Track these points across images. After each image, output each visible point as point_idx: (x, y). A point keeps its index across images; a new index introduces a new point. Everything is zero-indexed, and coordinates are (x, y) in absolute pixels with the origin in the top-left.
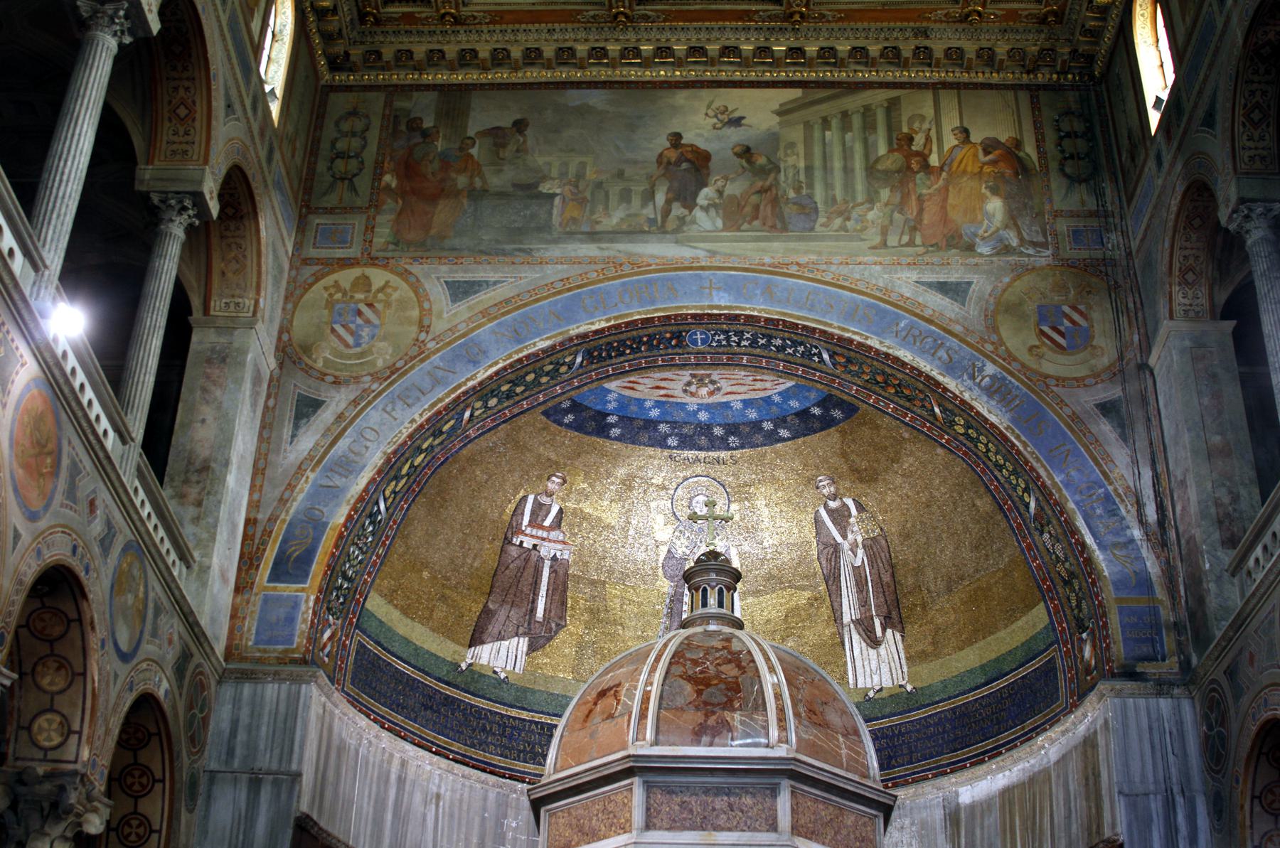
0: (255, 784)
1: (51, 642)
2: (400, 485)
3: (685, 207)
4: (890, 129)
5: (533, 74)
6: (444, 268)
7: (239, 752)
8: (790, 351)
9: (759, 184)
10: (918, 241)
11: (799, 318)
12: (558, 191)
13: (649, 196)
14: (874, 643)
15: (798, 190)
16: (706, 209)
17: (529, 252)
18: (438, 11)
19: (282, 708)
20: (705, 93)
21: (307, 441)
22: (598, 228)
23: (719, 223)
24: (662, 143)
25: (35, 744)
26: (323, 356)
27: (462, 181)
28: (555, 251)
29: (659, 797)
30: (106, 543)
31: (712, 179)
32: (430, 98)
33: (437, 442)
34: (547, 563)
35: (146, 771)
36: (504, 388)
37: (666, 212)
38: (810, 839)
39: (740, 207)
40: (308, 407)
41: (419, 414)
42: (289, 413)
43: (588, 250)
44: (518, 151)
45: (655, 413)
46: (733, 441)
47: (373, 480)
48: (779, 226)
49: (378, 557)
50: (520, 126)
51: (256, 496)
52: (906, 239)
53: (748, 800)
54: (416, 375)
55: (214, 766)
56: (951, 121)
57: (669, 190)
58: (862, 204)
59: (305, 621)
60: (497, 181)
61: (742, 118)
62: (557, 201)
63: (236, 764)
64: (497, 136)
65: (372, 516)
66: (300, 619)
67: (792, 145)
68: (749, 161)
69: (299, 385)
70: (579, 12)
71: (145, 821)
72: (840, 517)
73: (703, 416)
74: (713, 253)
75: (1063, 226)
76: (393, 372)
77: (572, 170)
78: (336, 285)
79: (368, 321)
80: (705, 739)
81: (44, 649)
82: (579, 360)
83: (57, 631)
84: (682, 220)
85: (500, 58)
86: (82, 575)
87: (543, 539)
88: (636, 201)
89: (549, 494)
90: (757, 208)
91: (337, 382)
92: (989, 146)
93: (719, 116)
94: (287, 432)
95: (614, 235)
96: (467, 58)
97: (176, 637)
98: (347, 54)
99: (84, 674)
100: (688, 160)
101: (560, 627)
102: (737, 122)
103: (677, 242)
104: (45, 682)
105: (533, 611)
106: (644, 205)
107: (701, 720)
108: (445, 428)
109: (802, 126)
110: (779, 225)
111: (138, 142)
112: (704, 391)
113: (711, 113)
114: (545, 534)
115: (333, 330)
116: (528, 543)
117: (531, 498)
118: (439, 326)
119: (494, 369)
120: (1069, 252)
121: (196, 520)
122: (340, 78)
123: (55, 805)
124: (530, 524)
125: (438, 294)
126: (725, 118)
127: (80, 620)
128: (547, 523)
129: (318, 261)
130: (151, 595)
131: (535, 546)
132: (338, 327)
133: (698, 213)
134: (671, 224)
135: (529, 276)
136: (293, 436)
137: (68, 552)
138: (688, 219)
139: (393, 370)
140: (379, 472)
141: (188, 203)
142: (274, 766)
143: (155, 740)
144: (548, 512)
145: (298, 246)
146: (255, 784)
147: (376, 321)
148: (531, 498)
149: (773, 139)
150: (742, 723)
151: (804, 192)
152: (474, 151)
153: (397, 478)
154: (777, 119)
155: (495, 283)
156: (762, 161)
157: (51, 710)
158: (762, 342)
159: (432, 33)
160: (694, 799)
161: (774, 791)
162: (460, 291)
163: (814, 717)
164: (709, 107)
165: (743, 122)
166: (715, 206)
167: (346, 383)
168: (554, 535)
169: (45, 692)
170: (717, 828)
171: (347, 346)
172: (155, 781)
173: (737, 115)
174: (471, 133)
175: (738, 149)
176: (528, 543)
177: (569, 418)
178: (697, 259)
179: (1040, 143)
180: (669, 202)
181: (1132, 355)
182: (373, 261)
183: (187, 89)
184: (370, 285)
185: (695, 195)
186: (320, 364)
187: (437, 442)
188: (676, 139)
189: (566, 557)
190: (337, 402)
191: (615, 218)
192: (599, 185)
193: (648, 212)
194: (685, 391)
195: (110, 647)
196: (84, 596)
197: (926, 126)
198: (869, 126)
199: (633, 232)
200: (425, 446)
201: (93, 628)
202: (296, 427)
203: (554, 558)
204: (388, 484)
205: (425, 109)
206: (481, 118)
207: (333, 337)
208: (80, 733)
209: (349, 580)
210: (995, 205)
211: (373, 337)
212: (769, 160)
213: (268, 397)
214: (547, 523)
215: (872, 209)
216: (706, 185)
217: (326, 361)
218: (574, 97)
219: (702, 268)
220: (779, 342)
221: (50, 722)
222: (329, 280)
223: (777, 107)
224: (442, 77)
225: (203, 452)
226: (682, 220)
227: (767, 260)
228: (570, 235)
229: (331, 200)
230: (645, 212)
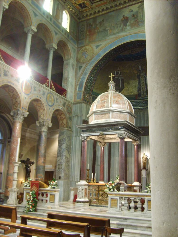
0: (78, 117)
1: (40, 106)
2: (94, 75)
5: (105, 12)
6: (95, 44)
7: (76, 113)
8: (142, 44)
9: (135, 20)
11: (142, 39)
12: (108, 29)
13: (120, 26)
15: (141, 19)
16: (128, 26)
17: (105, 39)
18: (89, 8)
19: (80, 107)
20: (128, 8)
21: (81, 72)
22: (114, 33)
23: (130, 28)
24: (122, 17)
25: (41, 118)
26: (82, 60)
27: (96, 31)
28: (109, 38)
29: (96, 116)
30: (44, 94)
31: (129, 21)
32: (92, 20)
33: (98, 68)
34: (120, 80)
35: (63, 118)
36: (105, 59)
37: (123, 28)
38: (115, 119)
40: (81, 67)
42: (78, 69)
43: (113, 36)
44: (103, 24)
45: (129, 56)
46: (141, 58)
47: (89, 75)
49: (93, 84)
50: (103, 20)
51: (76, 80)
53: (106, 115)
54: (93, 60)
55: (73, 115)
57: (123, 25)
59: (82, 95)
60: (101, 30)
62: (109, 30)
63: (76, 114)
64: (100, 23)
65: (91, 80)
66: (82, 95)
67: (140, 12)
68: (134, 17)
69: (80, 65)
70: (107, 2)
71: (64, 123)
73: (136, 55)
74: (129, 33)
76: (90, 60)
77: (110, 25)
78: (83, 50)
79: (86, 54)
80: (102, 108)
81: (39, 107)
82: (114, 52)
83: (40, 105)
84: (125, 29)
85: (99, 12)
86: (40, 99)
87: (119, 77)
89: (118, 70)
90: (135, 24)
91: (84, 63)
93: (130, 11)
94: (78, 71)
95: (116, 33)
96: (95, 13)
97: (62, 101)
98: (80, 17)
99: (44, 109)
100: (125, 19)
101: (123, 88)
102: (132, 11)
103: (125, 32)
104: (41, 111)
105: (119, 86)
106: (120, 28)
107: (101, 105)
108: (98, 66)
109: (141, 9)
110: (138, 26)
111: (46, 42)
112: (134, 52)
113: (128, 11)
114: (119, 76)
115: (83, 56)
116: (117, 78)
117: (116, 72)
118: (95, 52)
119: (102, 57)
121: (66, 86)
122: (80, 20)
123: (44, 125)
124: (117, 75)
125: (95, 48)
126: (130, 11)
127: (42, 104)
128: (119, 74)
129: (80, 47)
130: (55, 98)
131: (118, 78)
132: (83, 56)
133: (127, 27)
134: (123, 30)
135: (106, 42)
136: (79, 71)
137: (36, 97)
139: (90, 60)
140: (90, 74)
141: (52, 48)
142: (80, 115)
143: (62, 114)
144: (119, 73)
145: (78, 46)
146: (78, 117)
147: (87, 54)
148: (116, 72)
149: (137, 12)
150: (106, 105)
151: (142, 19)
152: (98, 26)
153: (93, 74)
154: (138, 9)
155: (102, 44)
156: (136, 16)
157: (42, 114)
158: (138, 44)
159: (90, 11)
160: (100, 115)
161: (109, 113)
162: (97, 47)
163: (117, 103)
164: (128, 10)
165: (133, 11)
166: (129, 25)
167: (85, 63)
168: (120, 76)
169: (41, 112)
170: (103, 119)
171: (84, 58)
172: (64, 119)
173: (132, 10)
174: (97, 23)
175: (132, 15)
177: (117, 60)
178: (127, 34)
180: (123, 26)
182: (87, 45)
183: (49, 34)
184: (86, 49)
185: (127, 25)
186: (81, 61)
187: (98, 68)
188: (124, 16)
189: (123, 78)
190: (84, 66)
191: (116, 31)
192: (114, 26)
193: (121, 29)
194: (132, 52)
195: (48, 106)
196: (41, 101)
199: (119, 32)
200: (96, 69)
201: (44, 104)
202: (79, 70)
203: (121, 79)
204: (92, 75)
205: (91, 22)
206: (99, 20)
207: (83, 57)
208: (45, 116)
209: (89, 88)
211: (87, 56)
212: (137, 16)
213: (76, 67)
214: (119, 74)
216: (128, 22)
217: (82, 60)
218: (110, 14)
219: (128, 35)
220: (140, 43)
221: (42, 115)
222: (81, 50)
223: (137, 7)
224: (92, 16)
225: (66, 77)
227: (137, 31)
228: (110, 35)
230: (120, 29)
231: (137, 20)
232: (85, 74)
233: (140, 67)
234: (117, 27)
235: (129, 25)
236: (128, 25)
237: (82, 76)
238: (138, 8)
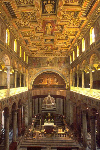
4: (58, 60)
13: (46, 64)
26: (31, 74)
41: (36, 77)
48: (52, 66)
50: (39, 60)
56: (61, 59)
69: (30, 75)
72: (55, 77)
75: (66, 66)
92: (63, 61)
120: (66, 67)
162: (37, 70)
181: (69, 73)
182: (33, 68)
190: (32, 76)
210: (63, 64)
229: (30, 65)
232: (33, 80)
233: (49, 76)
234: (45, 64)
237: (31, 80)
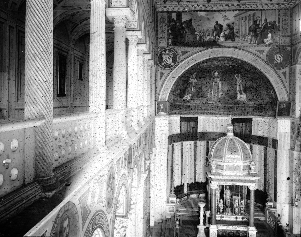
3: (218, 36)
10: (256, 42)
12: (198, 34)
14: (241, 94)
16: (222, 37)
39: (228, 36)
52: (254, 42)
58: (247, 35)
61: (228, 18)
68: (229, 27)
88: (210, 36)
102: (227, 19)
106: (212, 36)
133: (221, 38)
138: (219, 39)
154: (234, 18)
155: (189, 52)
166: (224, 36)
174: (183, 22)
175: (227, 25)
176: (191, 81)
179: (279, 22)
180: (216, 36)
188: (217, 22)
197: (260, 19)
198: (250, 20)
215: (249, 36)
226: (218, 39)
231: (231, 33)
235: (224, 36)
236: (221, 35)
238: (235, 17)
